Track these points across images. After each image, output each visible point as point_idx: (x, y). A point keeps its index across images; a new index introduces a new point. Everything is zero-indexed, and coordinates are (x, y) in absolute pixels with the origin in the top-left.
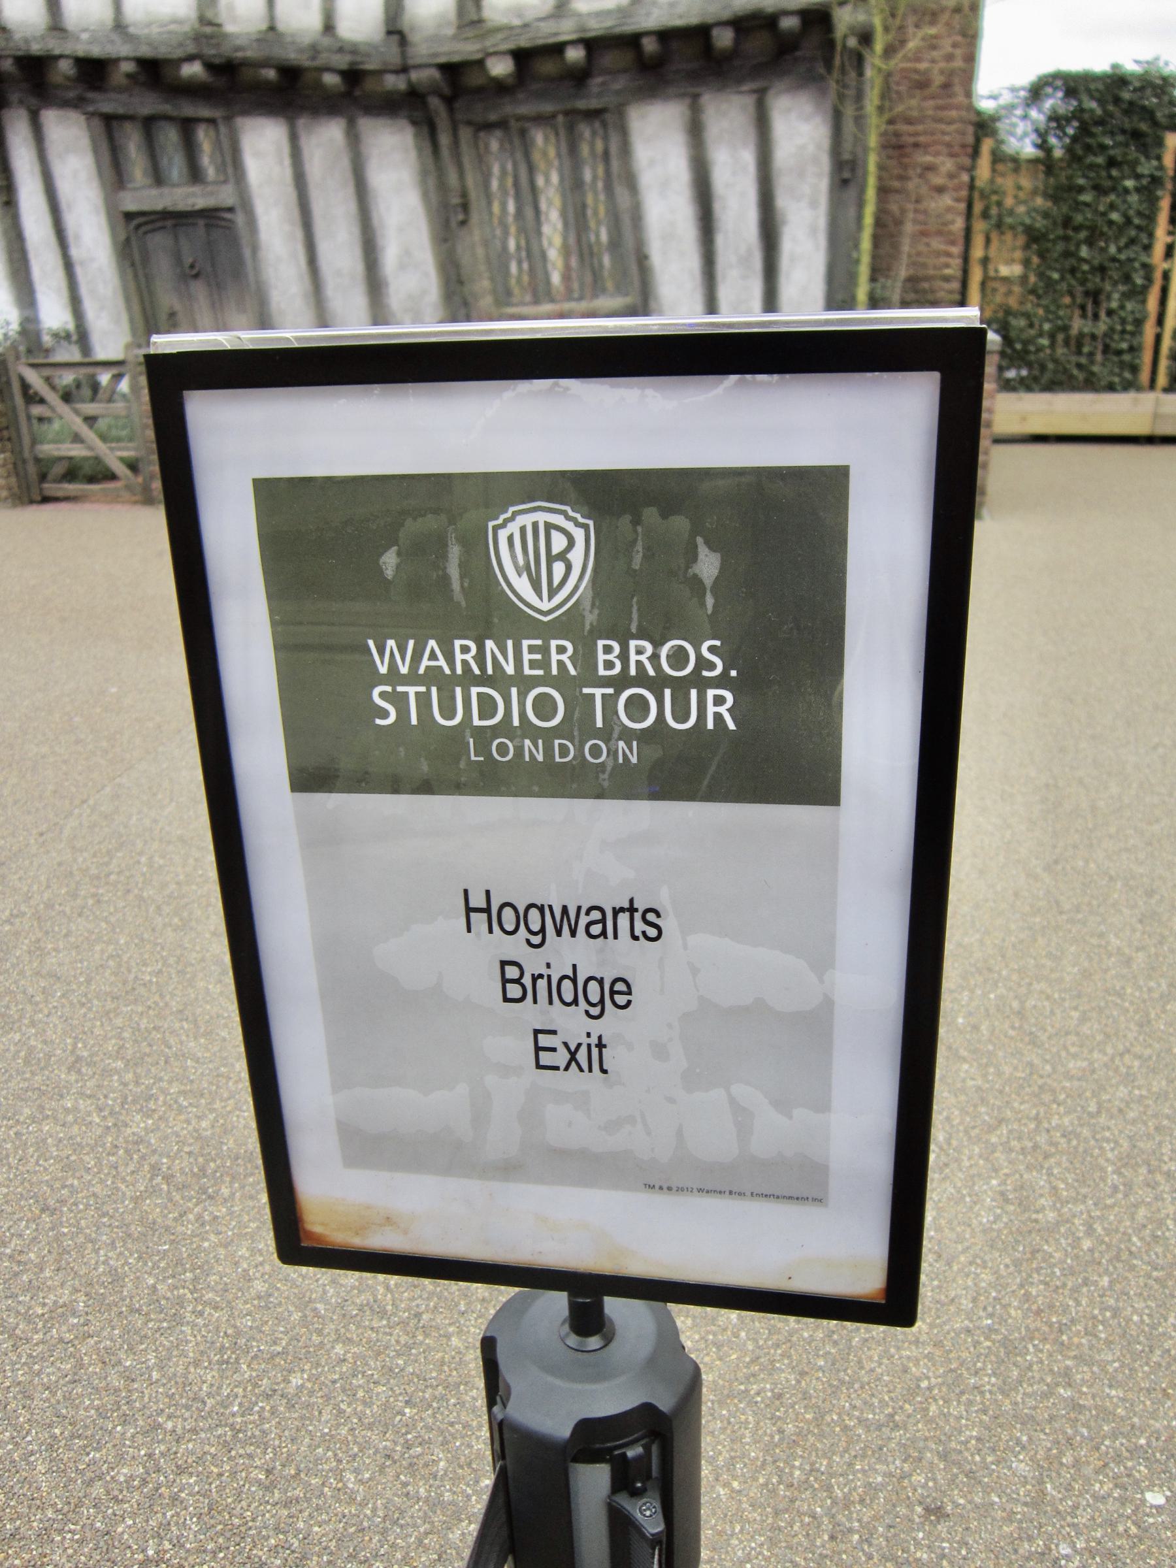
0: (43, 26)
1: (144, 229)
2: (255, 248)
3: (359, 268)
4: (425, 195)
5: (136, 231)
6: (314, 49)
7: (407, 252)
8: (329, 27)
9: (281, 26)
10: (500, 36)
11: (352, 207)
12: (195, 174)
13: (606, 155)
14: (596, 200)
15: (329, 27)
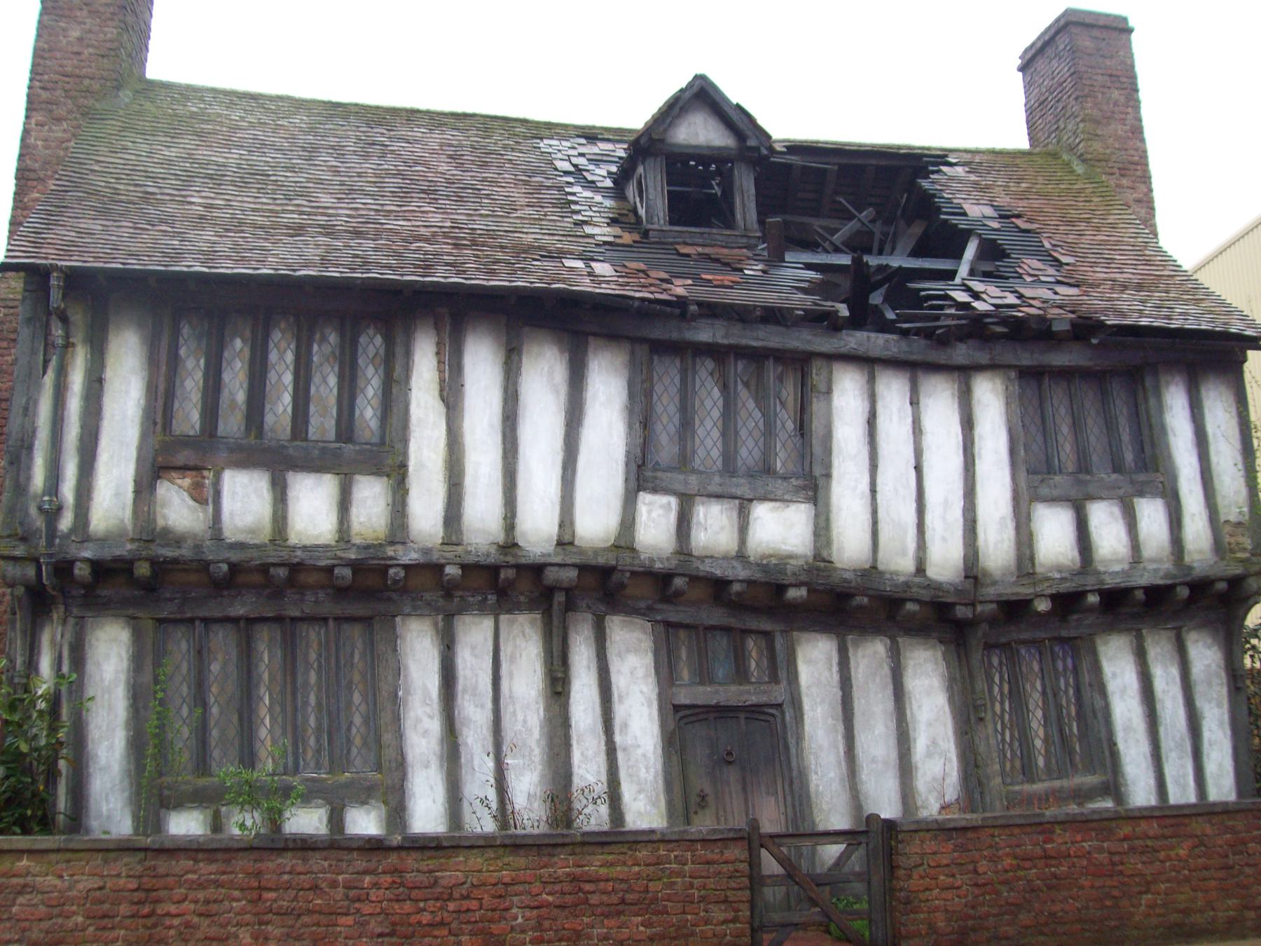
0: (671, 550)
1: (686, 720)
2: (800, 738)
3: (894, 755)
4: (951, 700)
5: (680, 722)
6: (907, 585)
7: (934, 742)
8: (920, 569)
9: (881, 567)
10: (1046, 584)
11: (890, 705)
12: (741, 674)
13: (1076, 670)
14: (1068, 701)
15: (920, 569)
